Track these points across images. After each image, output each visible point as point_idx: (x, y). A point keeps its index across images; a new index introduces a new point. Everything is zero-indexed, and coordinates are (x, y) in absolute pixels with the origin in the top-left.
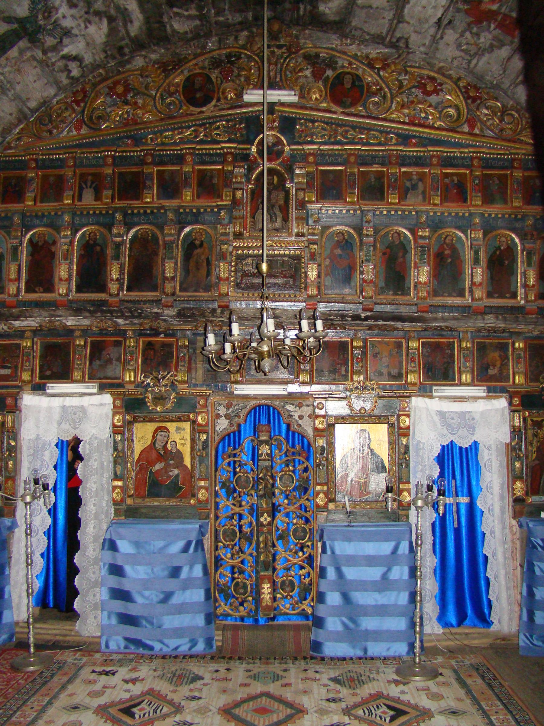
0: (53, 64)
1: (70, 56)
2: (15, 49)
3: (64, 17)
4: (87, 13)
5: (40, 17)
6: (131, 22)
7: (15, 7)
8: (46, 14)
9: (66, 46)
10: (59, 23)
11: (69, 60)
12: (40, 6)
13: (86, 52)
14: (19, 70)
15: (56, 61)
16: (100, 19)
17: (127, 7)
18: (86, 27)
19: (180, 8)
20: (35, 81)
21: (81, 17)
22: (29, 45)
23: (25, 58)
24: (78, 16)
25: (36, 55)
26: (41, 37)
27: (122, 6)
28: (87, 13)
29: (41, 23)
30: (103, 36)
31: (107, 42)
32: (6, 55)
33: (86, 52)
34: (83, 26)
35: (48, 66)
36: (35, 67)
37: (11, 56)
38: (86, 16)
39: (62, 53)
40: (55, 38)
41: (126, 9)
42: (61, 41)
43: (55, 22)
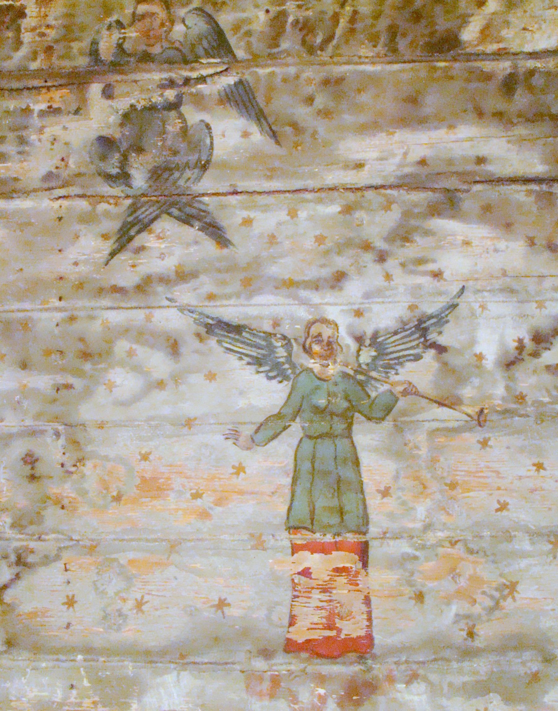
0: (521, 398)
1: (521, 347)
2: (365, 458)
3: (359, 313)
4: (382, 258)
5: (314, 365)
6: (481, 160)
7: (242, 403)
8: (316, 348)
9: (473, 342)
10: (369, 332)
11: (535, 354)
12: (281, 352)
13: (541, 305)
14: (453, 486)
15: (507, 388)
16: (427, 233)
17: (416, 155)
18: (437, 275)
19: (464, 20)
20: (539, 466)
21: (388, 277)
22: (388, 424)
23: (423, 452)
24: (379, 281)
25: (435, 425)
26: (383, 388)
27: (408, 170)
28: (382, 258)
29: (333, 370)
30: (502, 245)
31: (531, 242)
32: (370, 487)
33: (541, 305)
34: (425, 281)
35: (506, 412)
36: (484, 443)
37: (387, 481)
38: (391, 264)
39: (490, 362)
40: (417, 358)
41: (423, 162)
42: (441, 349)
43: (359, 339)
